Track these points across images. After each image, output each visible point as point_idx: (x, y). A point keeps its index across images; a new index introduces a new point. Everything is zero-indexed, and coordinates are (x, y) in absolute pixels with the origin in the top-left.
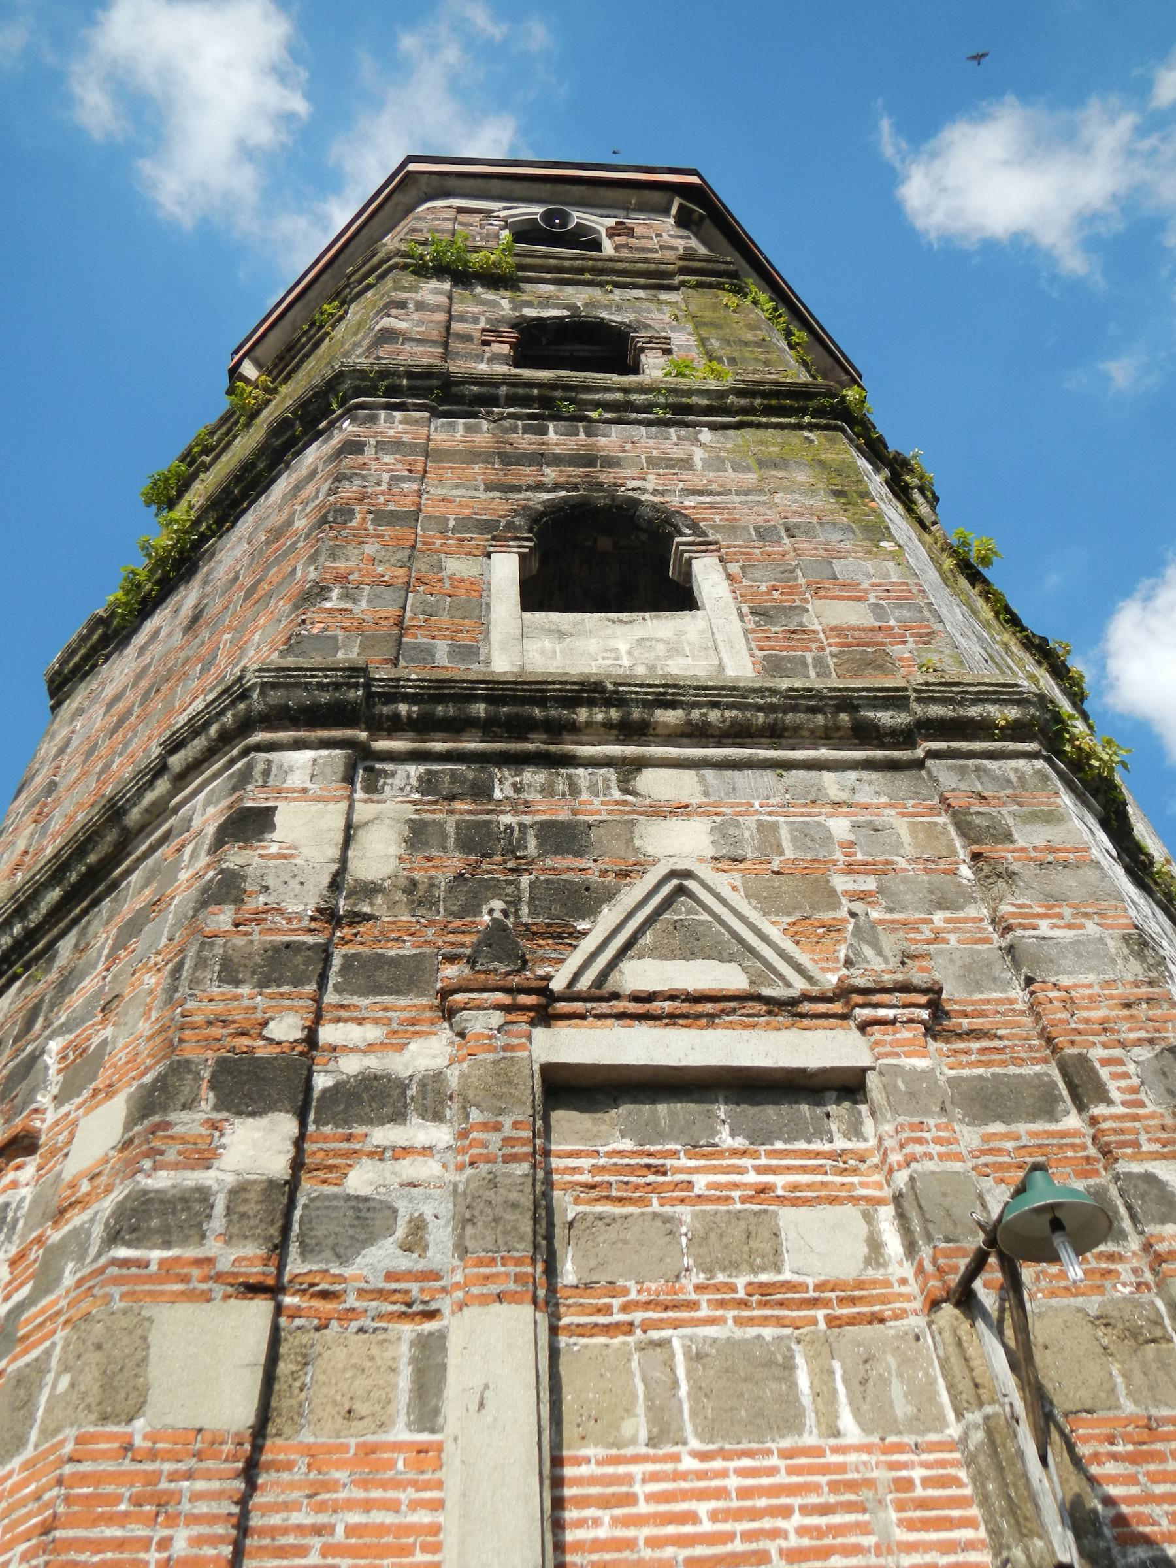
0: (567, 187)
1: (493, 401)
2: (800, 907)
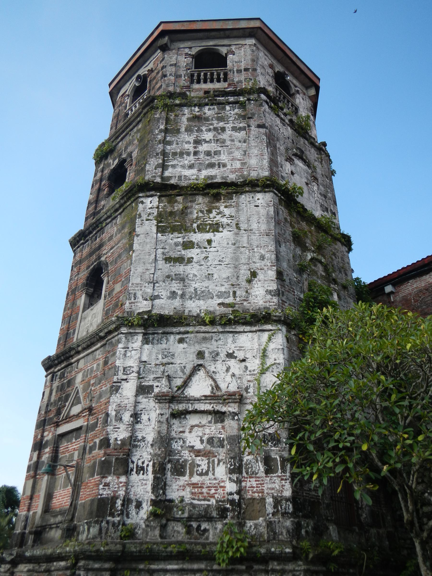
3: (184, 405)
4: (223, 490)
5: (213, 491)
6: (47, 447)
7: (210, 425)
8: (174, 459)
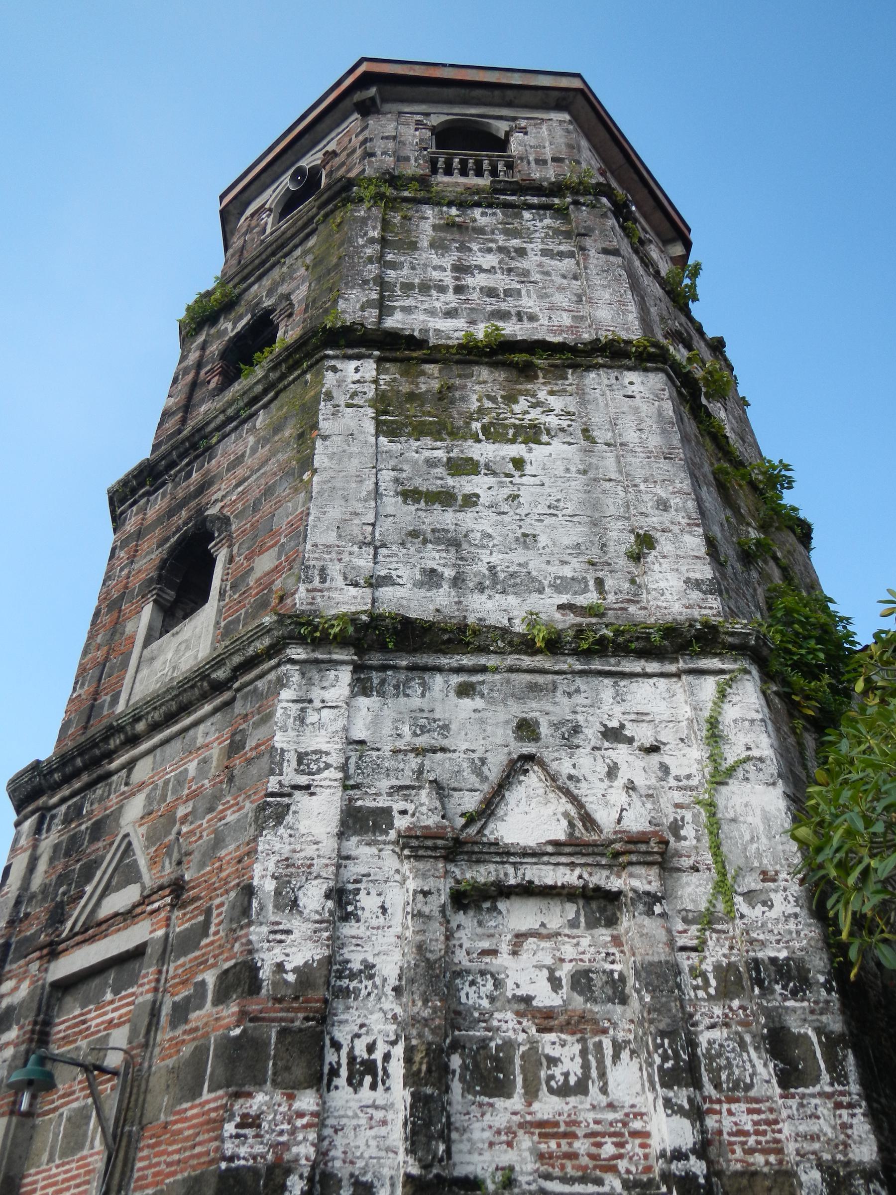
0: (299, 144)
2: (159, 839)
3: (492, 867)
4: (643, 1146)
5: (608, 1149)
6: (9, 1028)
7: (575, 932)
8: (471, 1038)
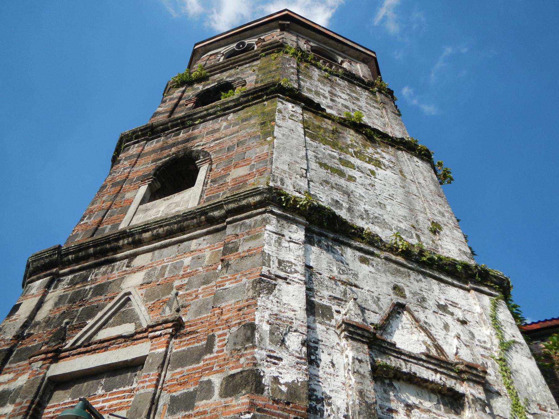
0: (244, 33)
1: (168, 129)
2: (158, 296)
